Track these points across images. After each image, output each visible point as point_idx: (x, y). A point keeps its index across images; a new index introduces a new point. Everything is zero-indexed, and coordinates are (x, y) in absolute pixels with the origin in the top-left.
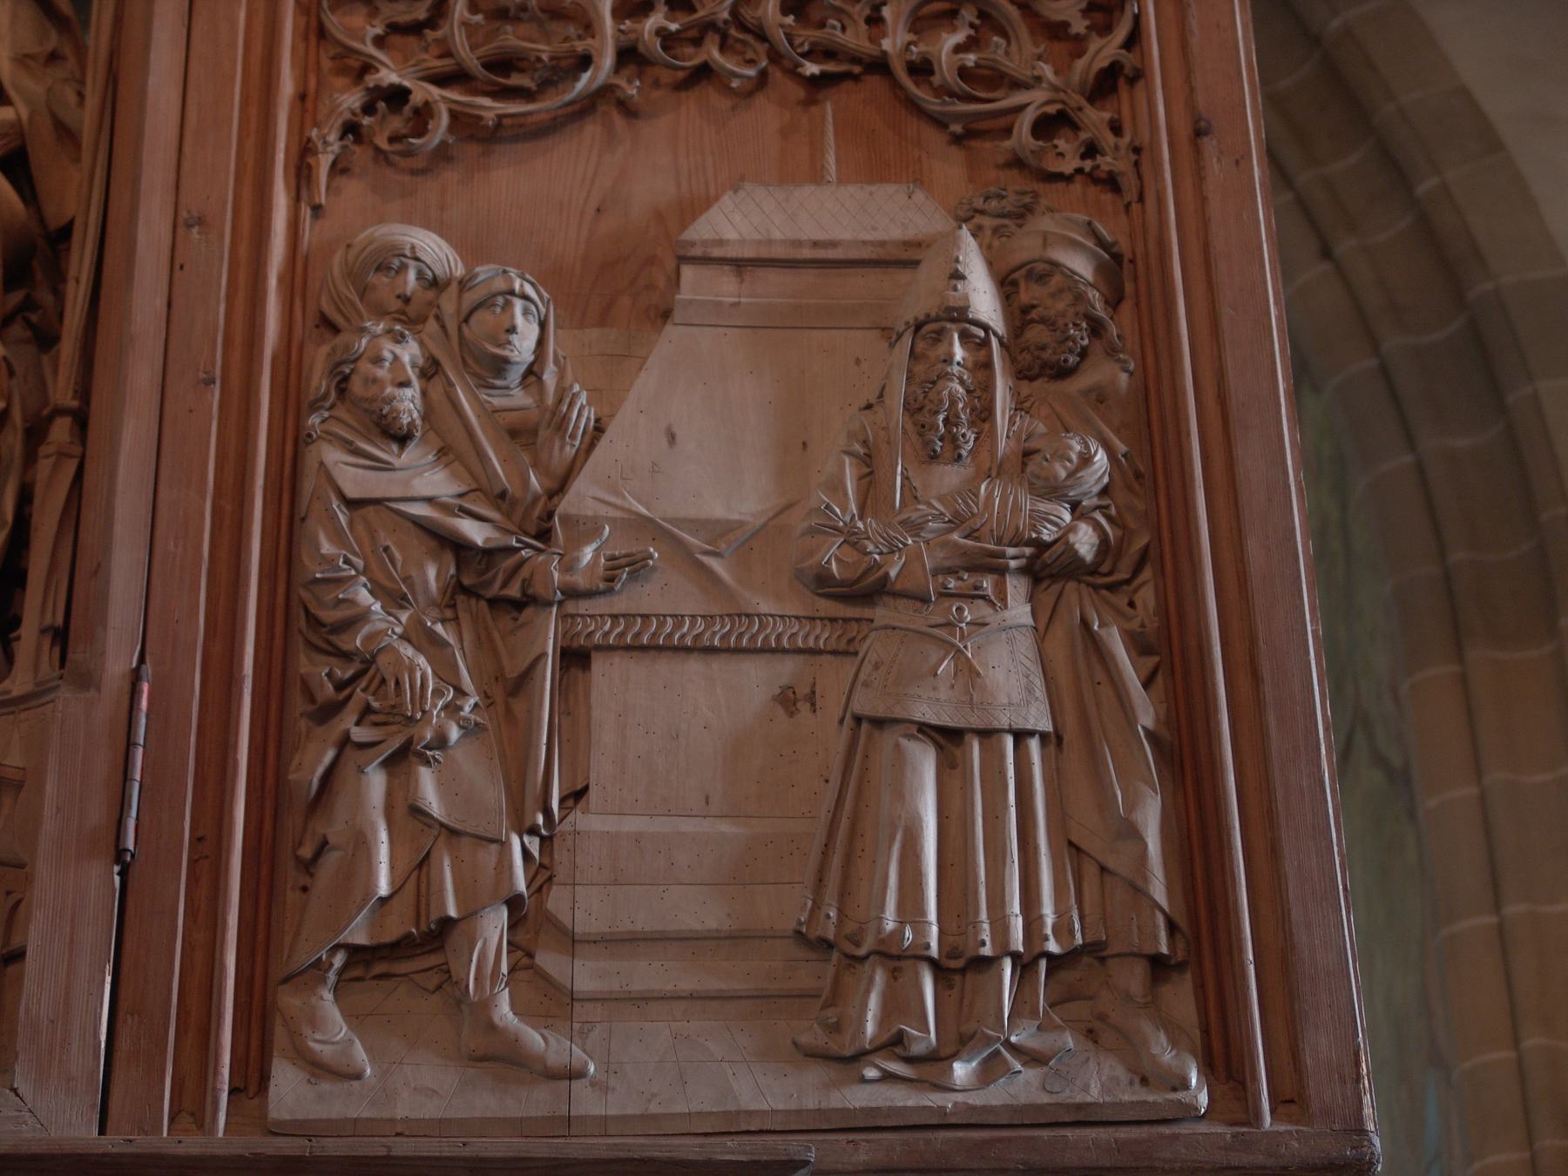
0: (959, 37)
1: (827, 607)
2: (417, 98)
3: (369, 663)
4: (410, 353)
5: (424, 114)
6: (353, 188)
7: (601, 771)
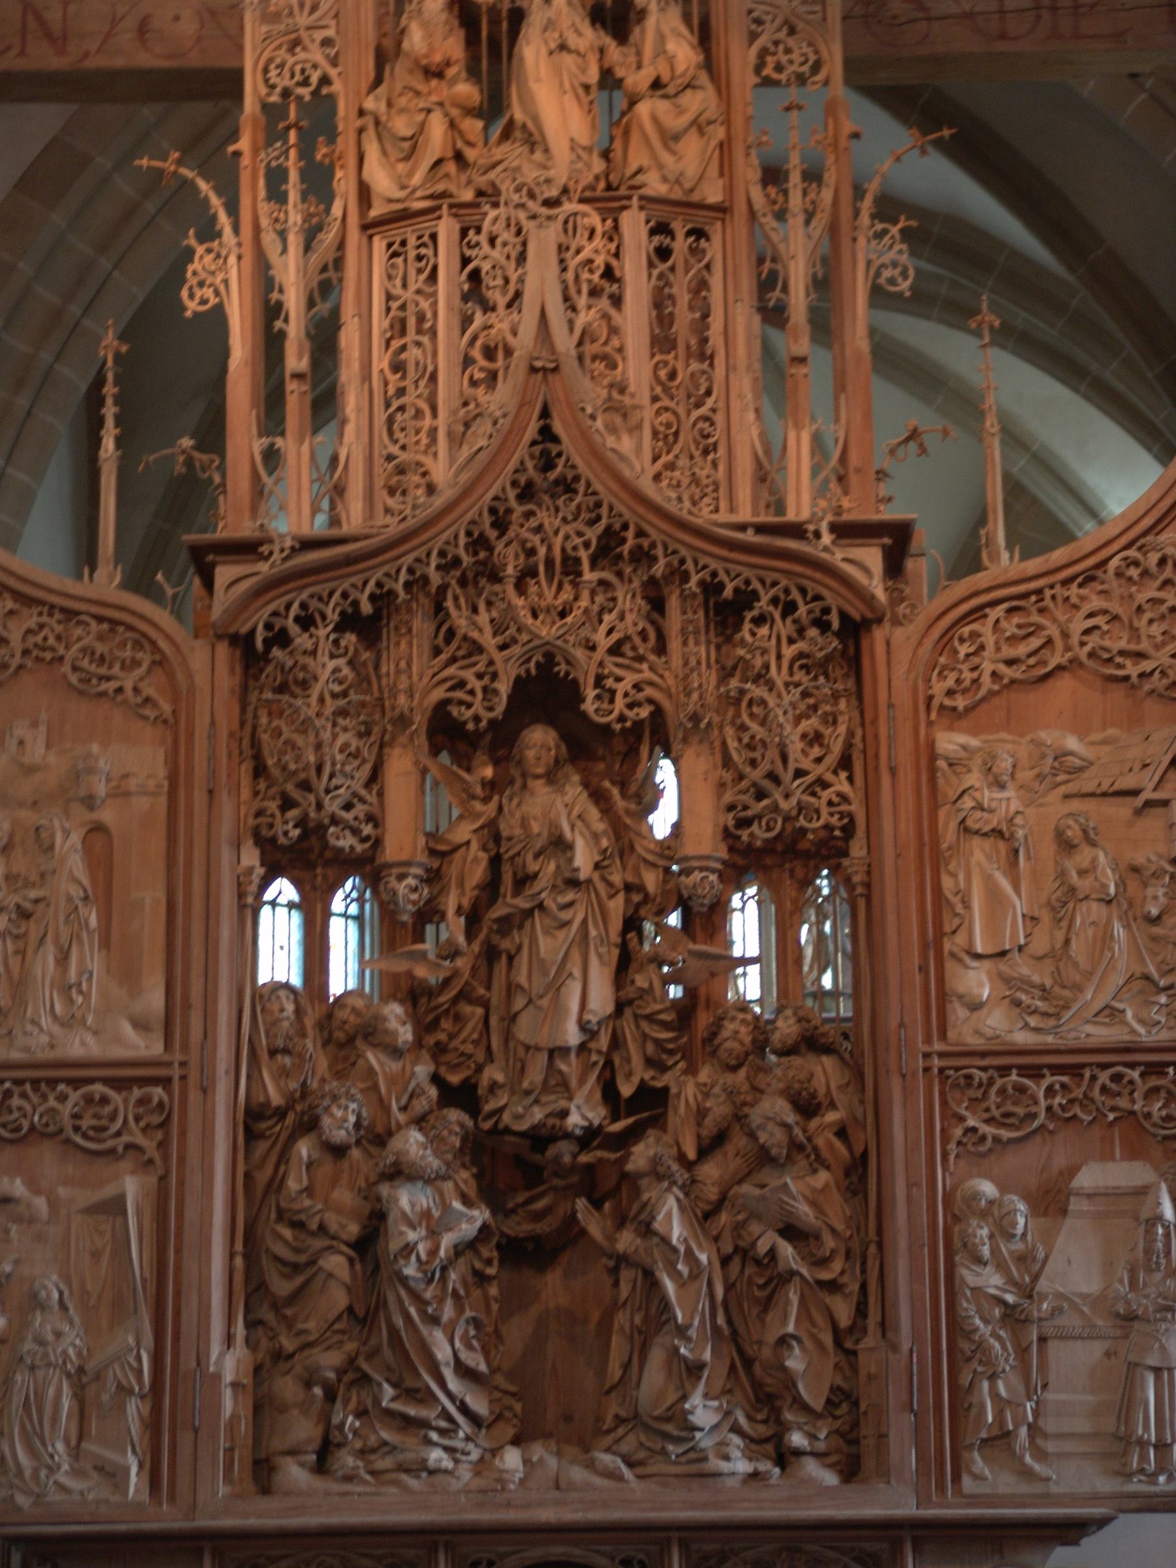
0: (1160, 1104)
1: (1119, 1322)
2: (980, 1132)
3: (980, 1345)
4: (984, 1232)
5: (983, 1138)
6: (962, 1163)
7: (1052, 1378)
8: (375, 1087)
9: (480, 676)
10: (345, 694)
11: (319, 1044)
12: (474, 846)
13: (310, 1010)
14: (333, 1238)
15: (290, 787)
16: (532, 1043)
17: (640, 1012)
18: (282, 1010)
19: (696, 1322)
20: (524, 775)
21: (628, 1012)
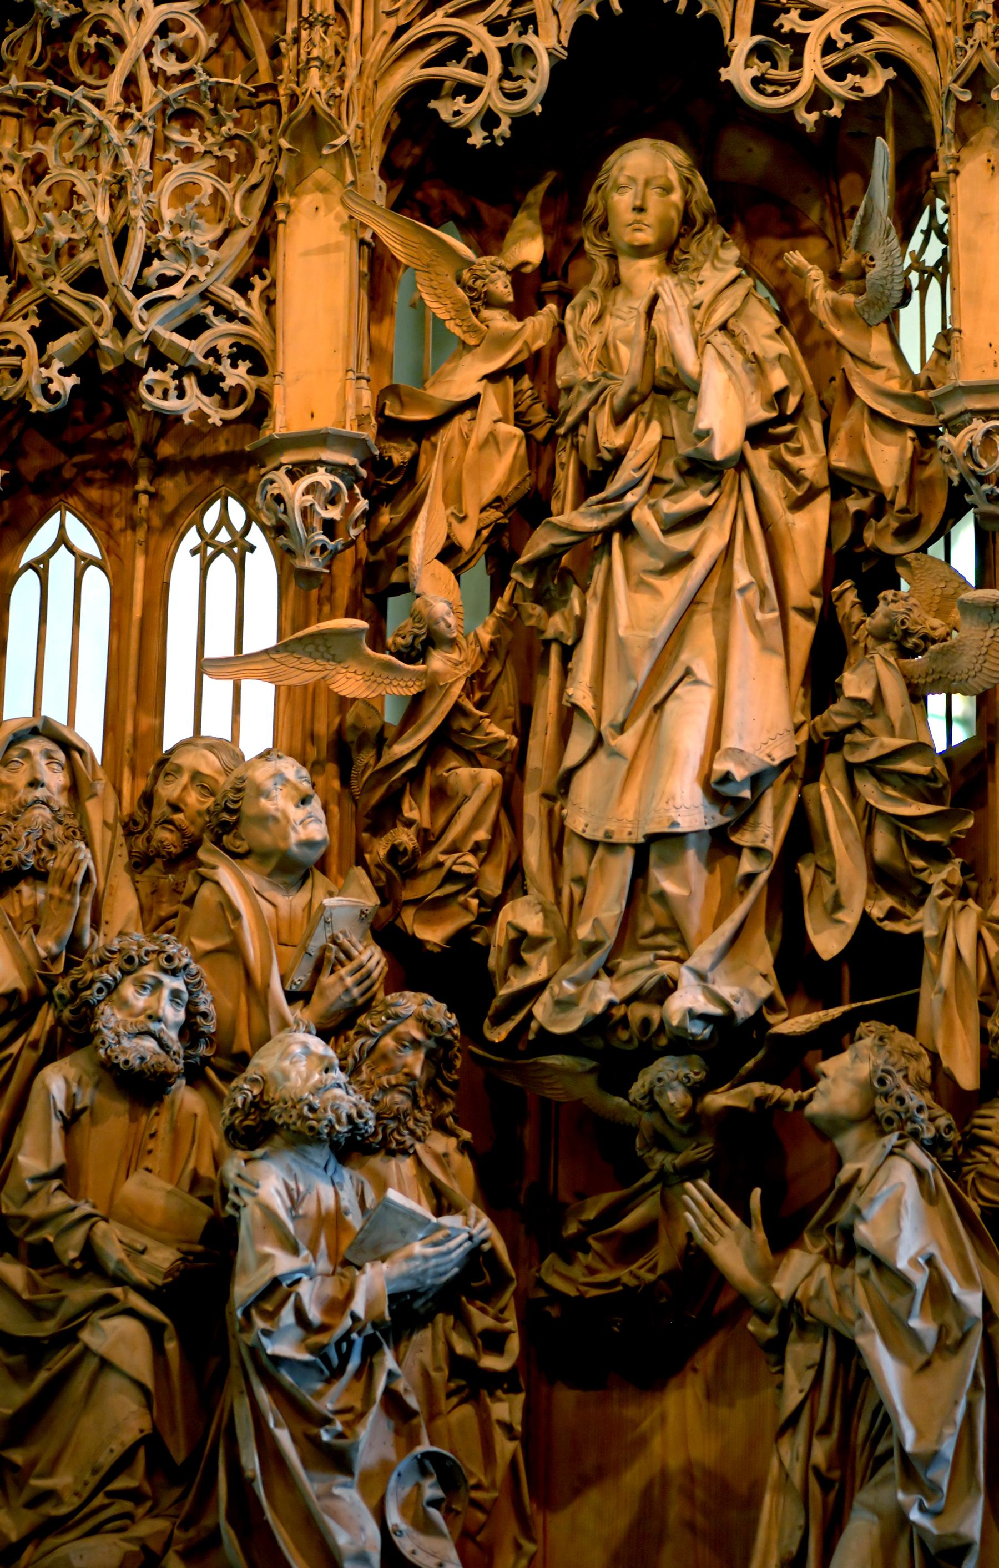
8: (235, 949)
9: (497, 27)
10: (188, 75)
11: (121, 859)
12: (491, 407)
13: (102, 785)
14: (118, 1281)
15: (58, 285)
16: (599, 836)
17: (855, 758)
18: (35, 783)
19: (948, 1449)
20: (613, 257)
21: (833, 765)
